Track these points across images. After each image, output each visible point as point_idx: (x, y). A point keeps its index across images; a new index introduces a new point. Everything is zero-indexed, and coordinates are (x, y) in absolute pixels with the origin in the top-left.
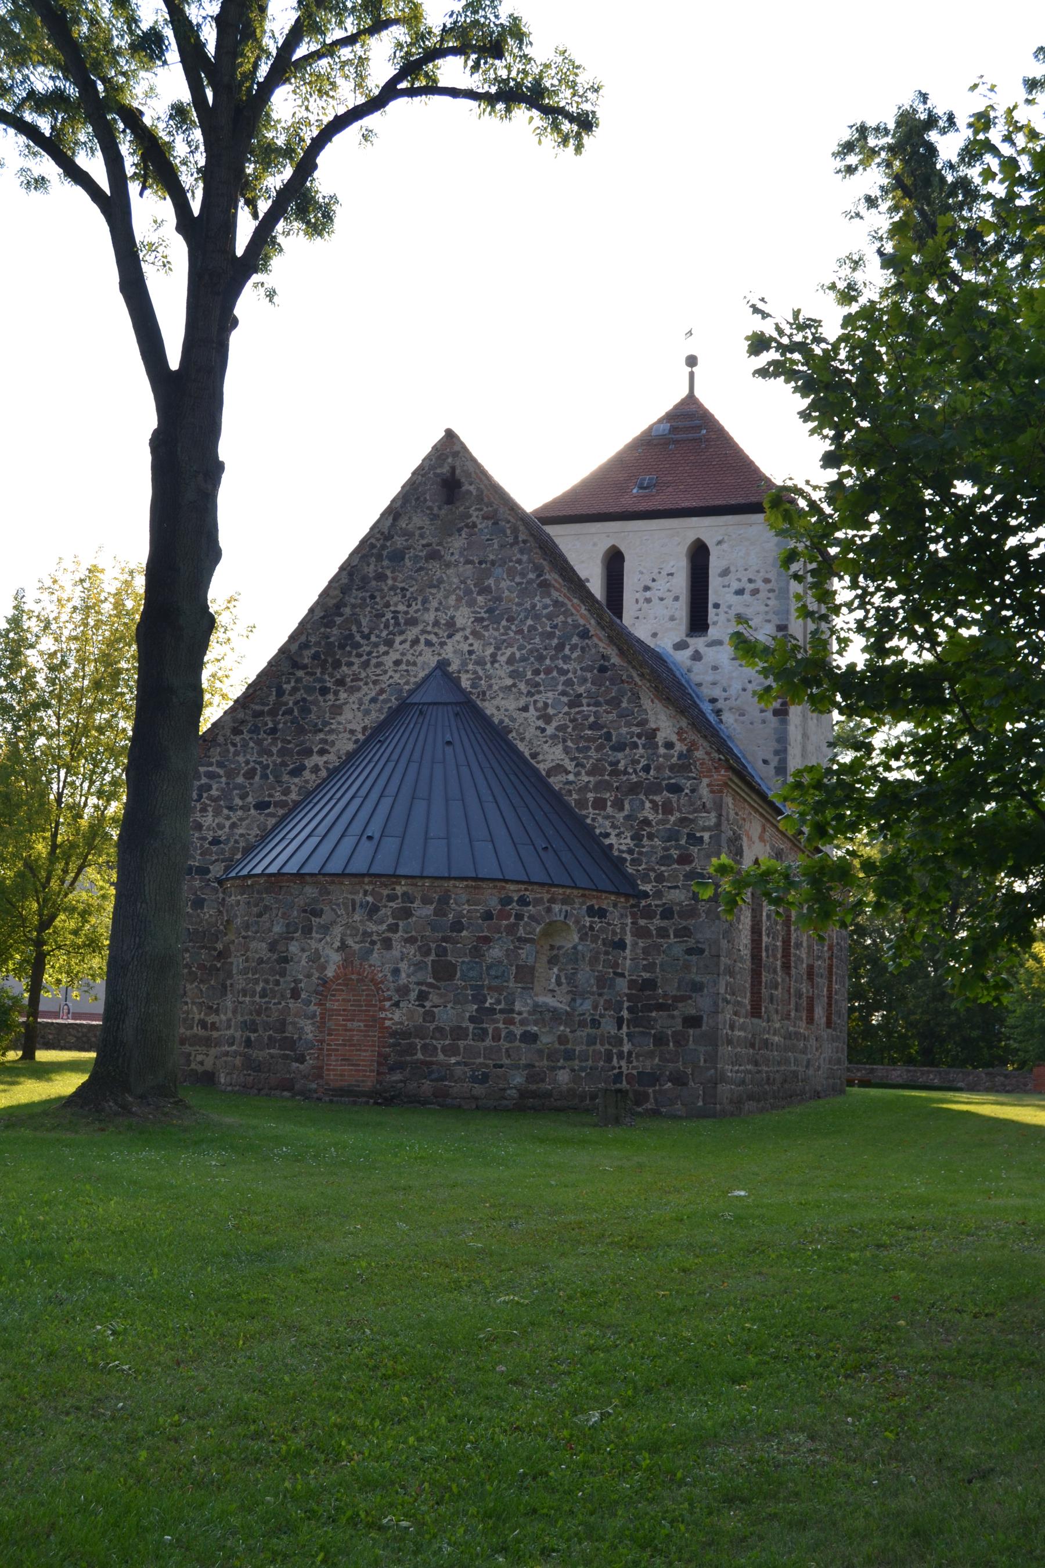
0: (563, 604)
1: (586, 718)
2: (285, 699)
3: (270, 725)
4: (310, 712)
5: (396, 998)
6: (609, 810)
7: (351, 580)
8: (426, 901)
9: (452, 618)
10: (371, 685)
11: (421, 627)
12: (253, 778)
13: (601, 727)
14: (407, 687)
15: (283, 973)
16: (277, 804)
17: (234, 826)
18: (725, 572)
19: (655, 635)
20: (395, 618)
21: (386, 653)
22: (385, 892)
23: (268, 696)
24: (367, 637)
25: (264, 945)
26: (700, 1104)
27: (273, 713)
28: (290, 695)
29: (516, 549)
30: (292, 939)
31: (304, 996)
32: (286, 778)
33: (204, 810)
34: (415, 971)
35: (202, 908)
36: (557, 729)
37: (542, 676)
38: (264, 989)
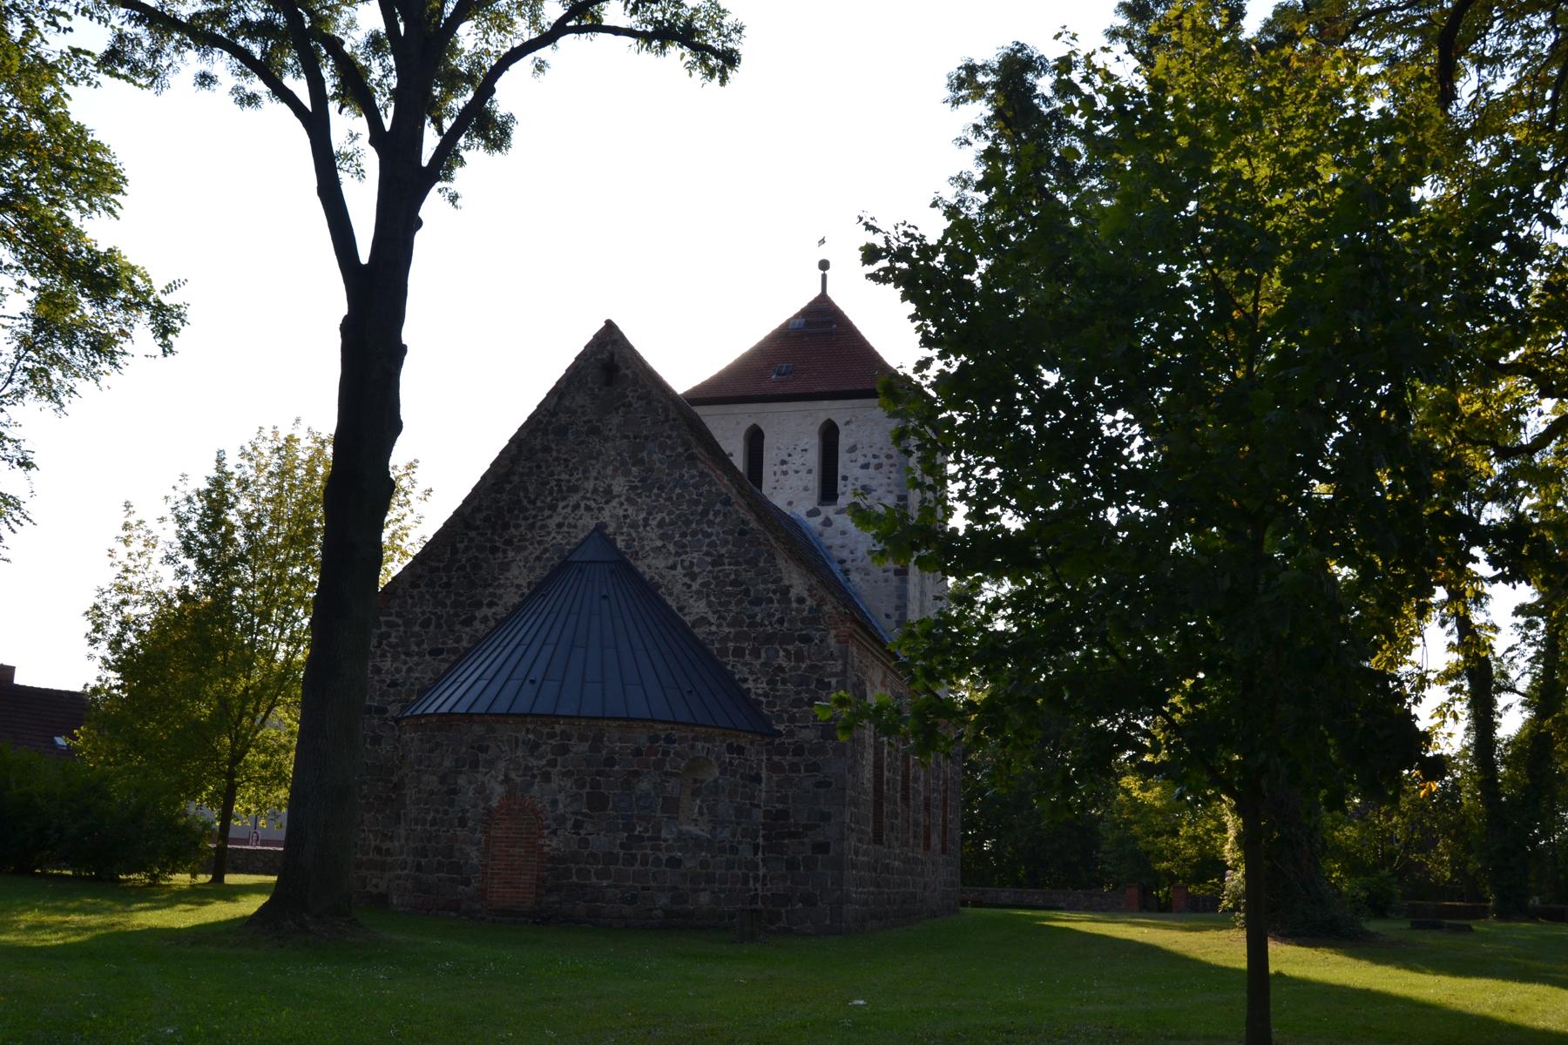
0: (708, 475)
5: (554, 826)
8: (582, 738)
9: (610, 486)
11: (581, 494)
17: (410, 670)
18: (853, 449)
19: (790, 503)
20: (559, 486)
21: (550, 517)
22: (546, 730)
24: (533, 502)
31: (470, 824)
32: (458, 627)
33: (383, 655)
36: (702, 585)
38: (434, 818)
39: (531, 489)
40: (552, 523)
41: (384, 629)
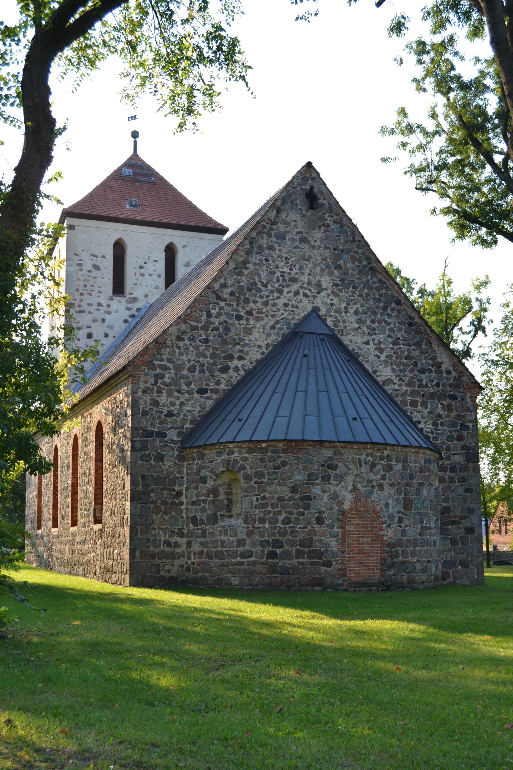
1: (403, 352)
2: (213, 319)
3: (204, 337)
4: (230, 330)
5: (388, 522)
6: (419, 407)
9: (319, 281)
10: (270, 317)
12: (194, 372)
13: (411, 358)
14: (293, 322)
16: (212, 391)
17: (182, 404)
21: (278, 298)
23: (201, 316)
24: (265, 286)
25: (286, 488)
26: (476, 577)
27: (205, 328)
28: (216, 317)
29: (354, 245)
30: (313, 484)
31: (327, 522)
33: (159, 391)
34: (396, 505)
35: (163, 461)
36: (387, 357)
37: (376, 324)
39: (263, 276)
40: (281, 302)
41: (158, 371)
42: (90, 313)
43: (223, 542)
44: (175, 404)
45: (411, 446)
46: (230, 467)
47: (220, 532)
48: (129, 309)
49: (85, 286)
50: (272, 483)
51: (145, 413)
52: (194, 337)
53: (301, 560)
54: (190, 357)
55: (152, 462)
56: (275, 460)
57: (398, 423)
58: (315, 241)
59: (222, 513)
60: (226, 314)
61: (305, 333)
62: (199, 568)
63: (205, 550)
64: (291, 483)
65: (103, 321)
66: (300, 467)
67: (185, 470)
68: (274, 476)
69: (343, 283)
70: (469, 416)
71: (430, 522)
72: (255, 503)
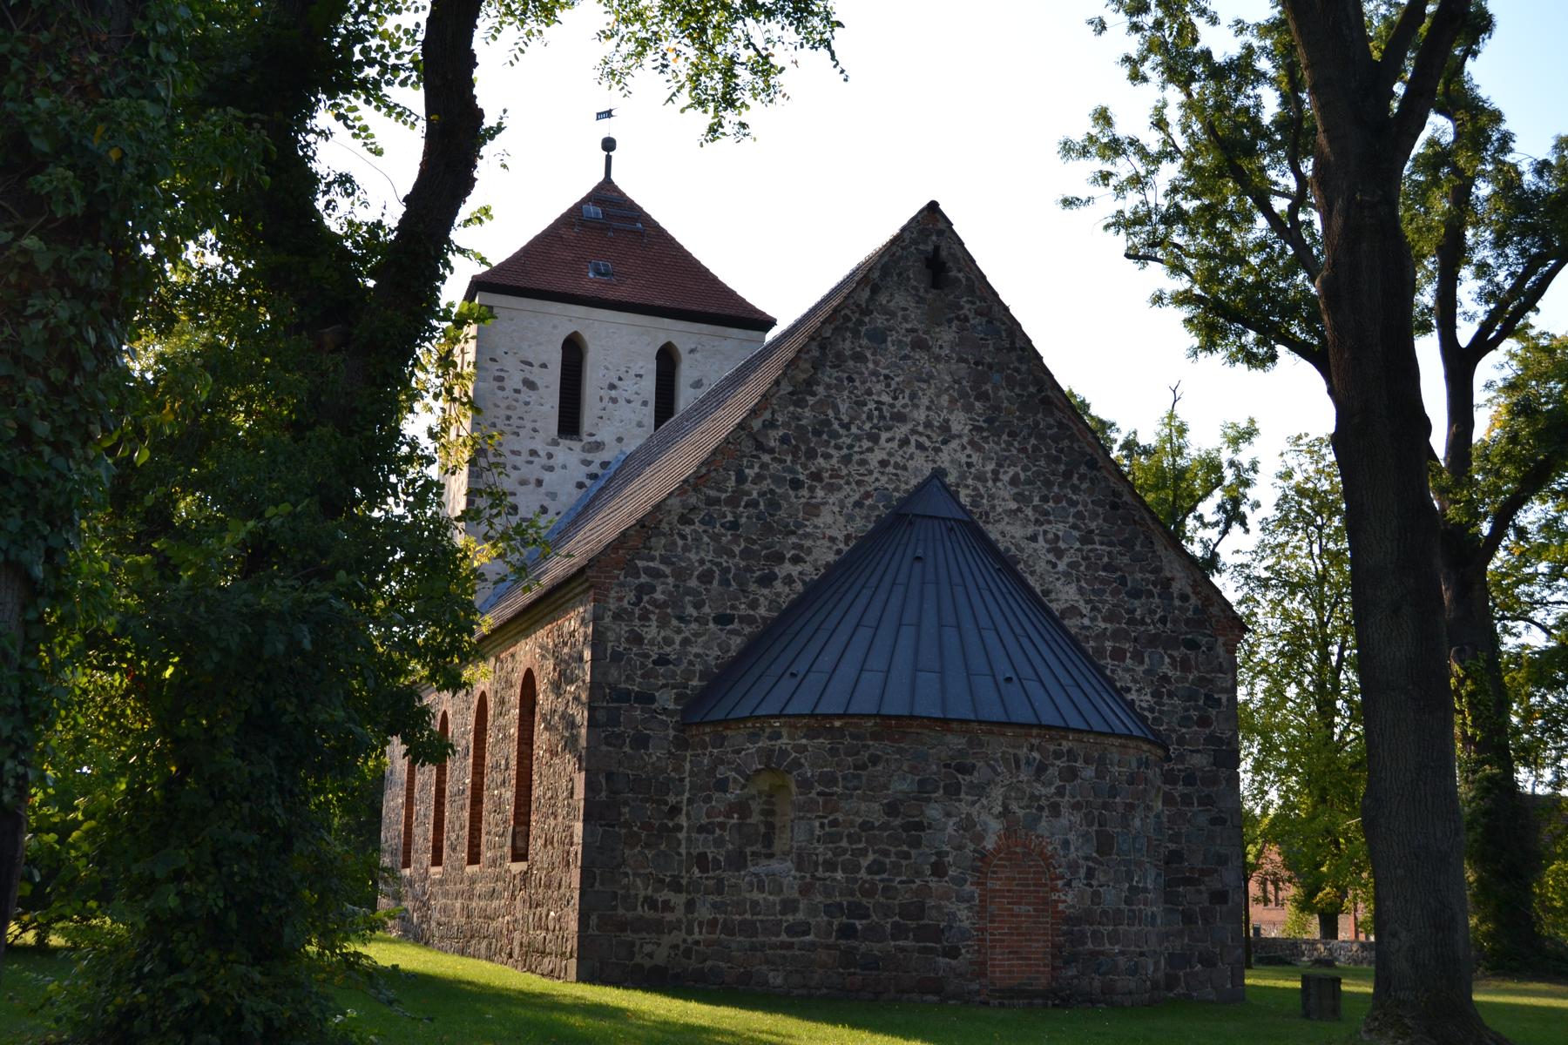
0: (1069, 428)
1: (1100, 557)
2: (747, 486)
3: (730, 518)
4: (779, 507)
5: (1068, 876)
7: (824, 354)
9: (947, 421)
10: (854, 486)
11: (910, 426)
12: (710, 583)
13: (1115, 570)
15: (916, 843)
16: (742, 619)
21: (870, 450)
22: (1052, 748)
24: (847, 427)
25: (876, 806)
27: (733, 502)
28: (754, 482)
29: (1013, 356)
30: (928, 800)
33: (644, 617)
36: (1069, 565)
37: (1051, 504)
39: (843, 408)
41: (644, 579)
42: (515, 468)
43: (755, 904)
44: (673, 642)
45: (1113, 735)
46: (772, 762)
47: (751, 884)
48: (587, 463)
49: (509, 418)
50: (851, 796)
51: (617, 657)
52: (711, 517)
53: (901, 943)
54: (702, 554)
55: (627, 749)
56: (858, 753)
57: (1088, 690)
58: (941, 347)
59: (754, 848)
60: (772, 476)
61: (917, 516)
62: (709, 951)
63: (721, 917)
64: (886, 796)
65: (539, 483)
66: (905, 767)
67: (687, 766)
68: (855, 782)
69: (992, 425)
70: (1222, 680)
71: (1145, 877)
72: (817, 832)
